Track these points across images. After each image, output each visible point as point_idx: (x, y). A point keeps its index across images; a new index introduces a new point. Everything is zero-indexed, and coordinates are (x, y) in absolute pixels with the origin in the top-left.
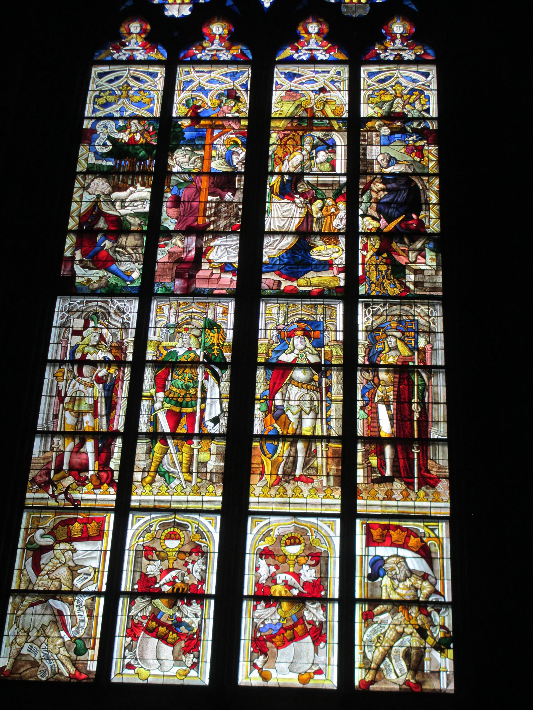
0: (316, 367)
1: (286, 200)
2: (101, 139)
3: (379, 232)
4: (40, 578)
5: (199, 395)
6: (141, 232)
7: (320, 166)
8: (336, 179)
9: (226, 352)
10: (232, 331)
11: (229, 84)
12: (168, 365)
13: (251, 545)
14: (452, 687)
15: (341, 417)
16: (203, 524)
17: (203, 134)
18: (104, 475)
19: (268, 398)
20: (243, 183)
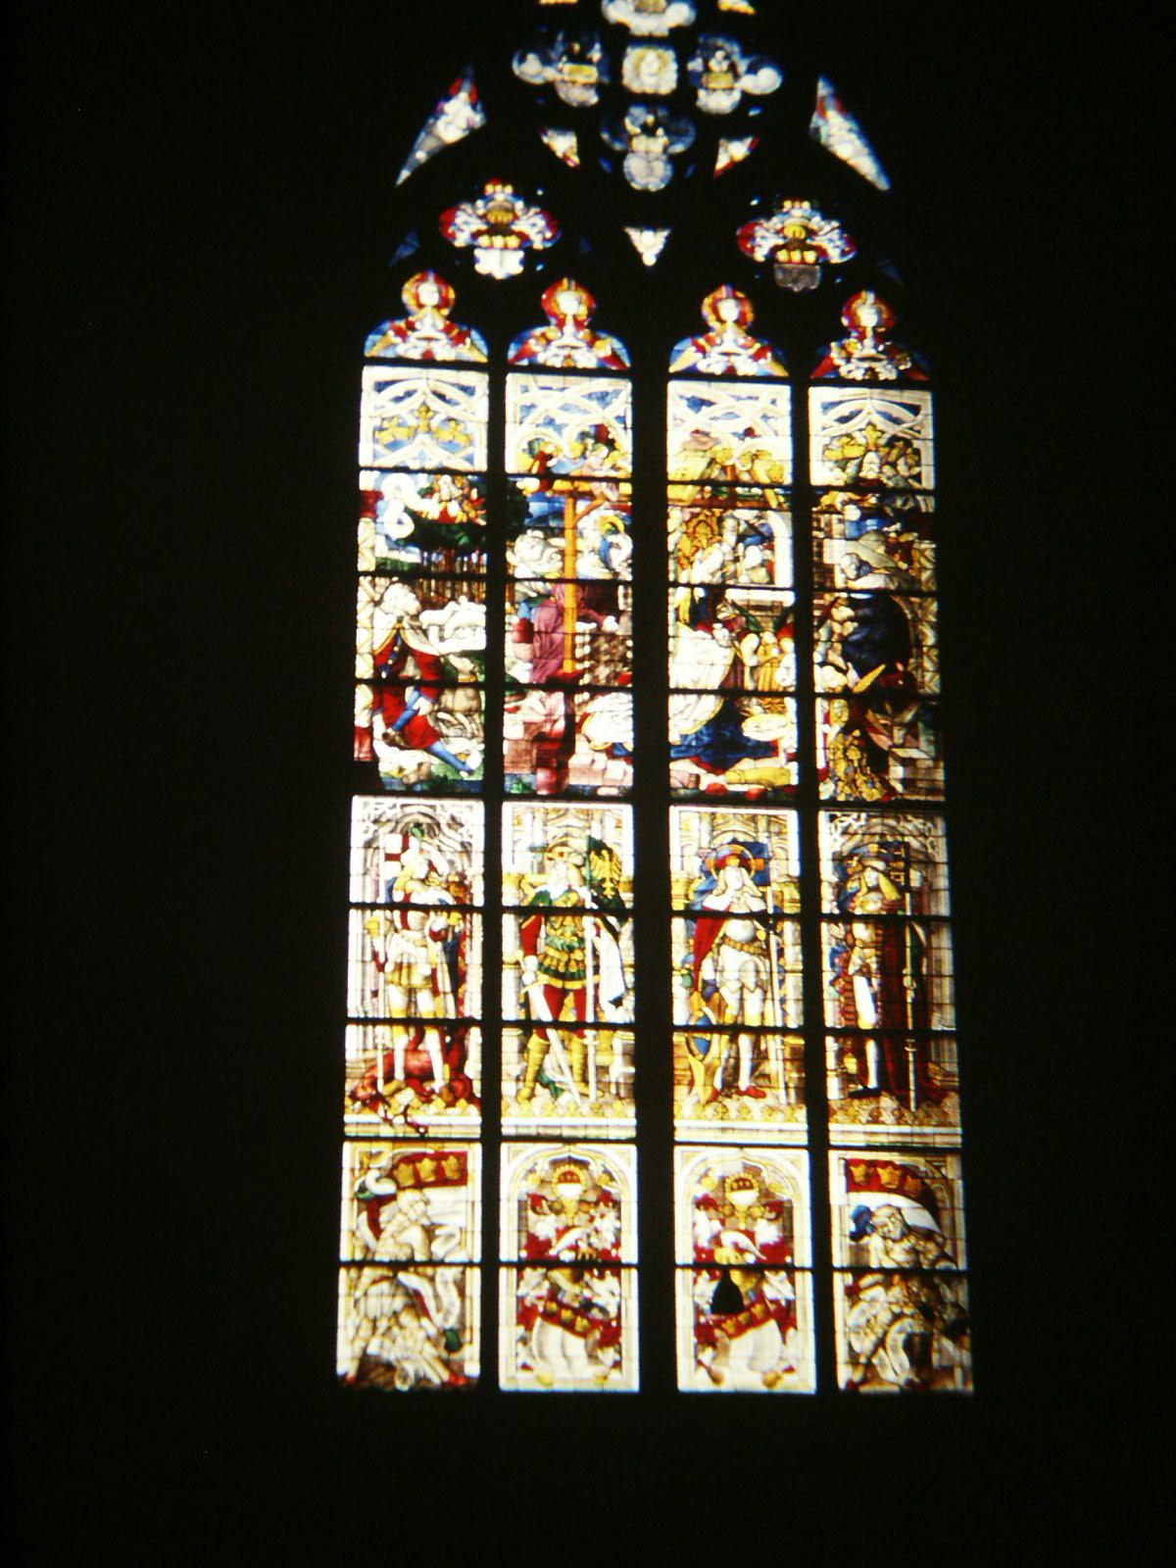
0: (761, 917)
3: (846, 693)
5: (589, 962)
6: (476, 686)
11: (598, 415)
12: (539, 911)
14: (970, 1387)
15: (801, 997)
18: (459, 1086)
20: (630, 600)
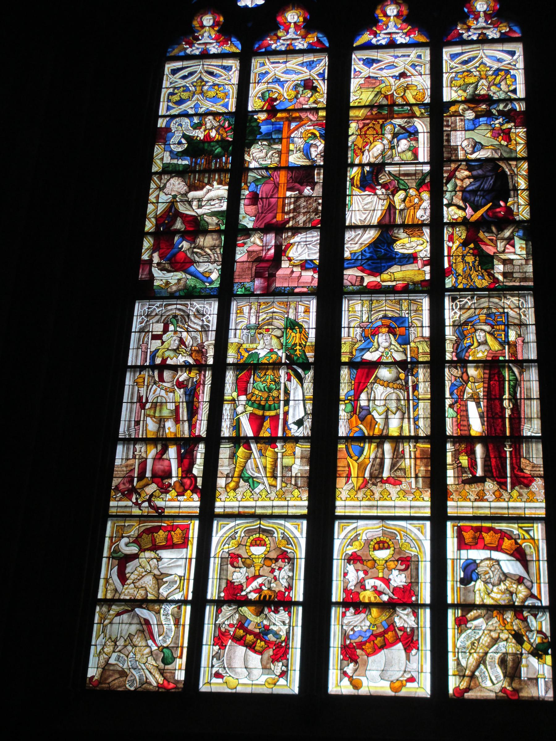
0: (402, 365)
1: (367, 193)
2: (176, 137)
3: (465, 222)
4: (125, 587)
5: (282, 397)
6: (219, 232)
7: (401, 155)
8: (419, 168)
9: (309, 352)
10: (314, 331)
11: (306, 73)
12: (249, 368)
13: (339, 550)
14: (550, 694)
15: (429, 416)
16: (289, 530)
17: (280, 128)
18: (187, 481)
19: (353, 399)
20: (322, 176)
